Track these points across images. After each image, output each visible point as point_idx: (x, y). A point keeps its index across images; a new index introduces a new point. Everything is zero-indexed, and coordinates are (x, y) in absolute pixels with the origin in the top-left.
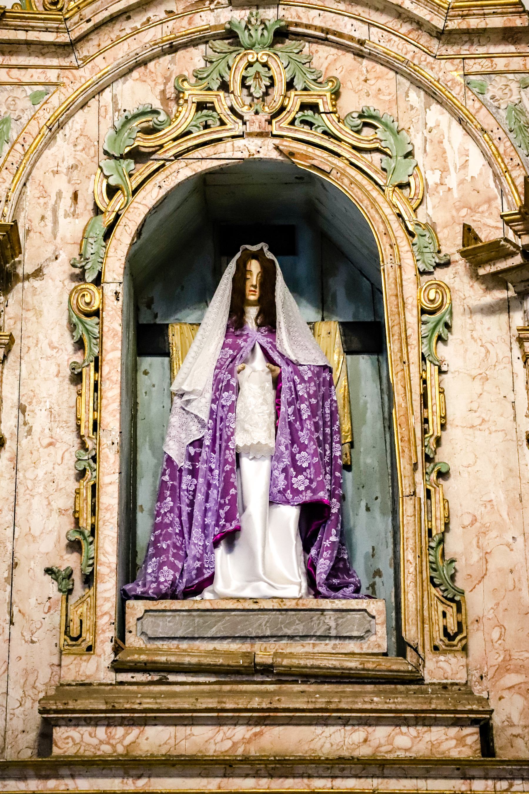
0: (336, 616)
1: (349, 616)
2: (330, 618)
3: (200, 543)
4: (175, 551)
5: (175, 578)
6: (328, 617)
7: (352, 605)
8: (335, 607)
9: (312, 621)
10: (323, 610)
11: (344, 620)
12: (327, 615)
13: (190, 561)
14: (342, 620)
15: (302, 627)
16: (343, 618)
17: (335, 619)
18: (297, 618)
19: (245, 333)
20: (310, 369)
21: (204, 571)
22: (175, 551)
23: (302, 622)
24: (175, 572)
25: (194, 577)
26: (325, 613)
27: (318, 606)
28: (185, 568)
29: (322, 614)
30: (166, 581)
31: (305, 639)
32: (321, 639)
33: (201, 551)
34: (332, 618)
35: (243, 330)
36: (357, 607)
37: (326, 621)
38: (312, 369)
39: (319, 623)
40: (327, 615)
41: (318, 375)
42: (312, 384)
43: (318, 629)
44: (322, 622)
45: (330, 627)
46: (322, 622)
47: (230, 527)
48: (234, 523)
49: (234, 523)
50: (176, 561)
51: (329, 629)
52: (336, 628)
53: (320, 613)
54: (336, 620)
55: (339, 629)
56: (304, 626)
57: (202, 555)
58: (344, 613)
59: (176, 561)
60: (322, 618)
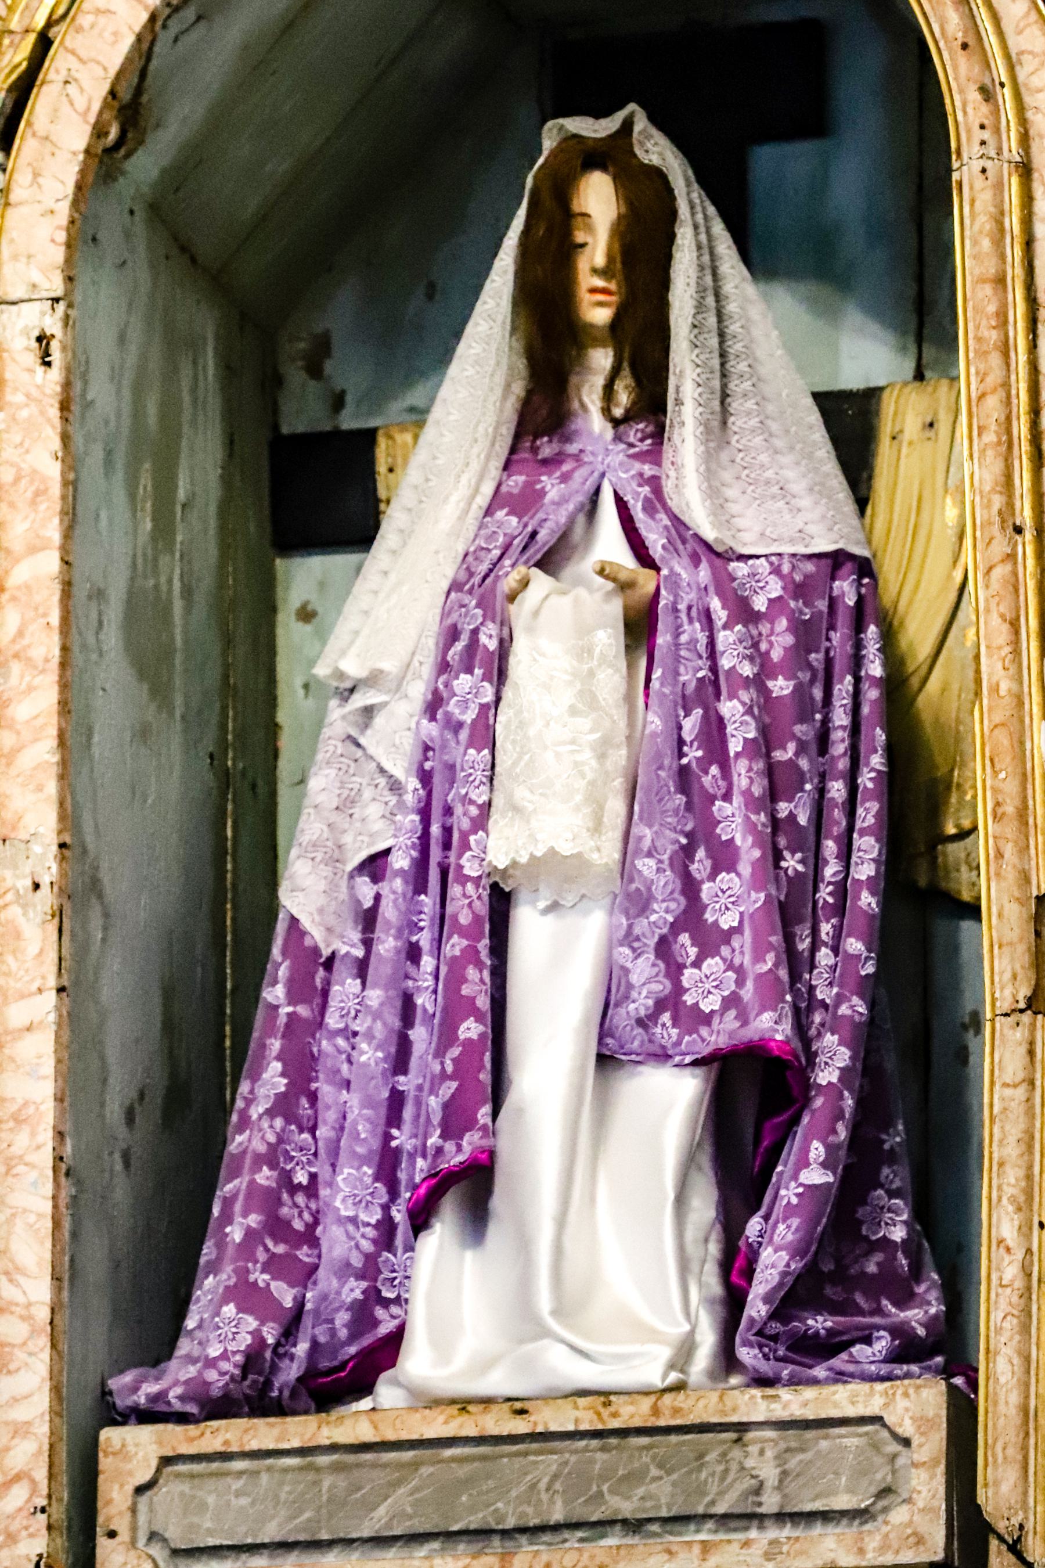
0: (783, 1445)
1: (824, 1444)
2: (762, 1452)
3: (363, 1217)
4: (280, 1249)
5: (259, 1342)
6: (753, 1449)
7: (836, 1405)
8: (779, 1412)
9: (699, 1468)
10: (742, 1427)
11: (808, 1456)
12: (754, 1441)
13: (326, 1279)
14: (801, 1456)
15: (668, 1489)
16: (802, 1450)
17: (777, 1457)
18: (654, 1458)
19: (572, 448)
20: (776, 571)
21: (380, 1313)
22: (280, 1249)
23: (669, 1473)
24: (263, 1323)
25: (343, 1333)
26: (751, 1435)
27: (724, 1413)
28: (309, 1306)
29: (738, 1441)
30: (224, 1356)
31: (677, 1527)
32: (733, 1524)
33: (367, 1246)
34: (769, 1454)
35: (567, 439)
36: (851, 1412)
37: (749, 1463)
38: (786, 568)
39: (726, 1471)
40: (754, 1441)
41: (800, 590)
42: (783, 623)
43: (721, 1493)
44: (734, 1467)
45: (761, 1484)
46: (734, 1467)
47: (455, 1158)
48: (471, 1141)
49: (471, 1141)
50: (273, 1285)
51: (758, 1491)
52: (779, 1488)
53: (732, 1435)
54: (781, 1459)
55: (791, 1487)
56: (674, 1484)
57: (371, 1260)
58: (810, 1434)
59: (273, 1285)
60: (736, 1453)
